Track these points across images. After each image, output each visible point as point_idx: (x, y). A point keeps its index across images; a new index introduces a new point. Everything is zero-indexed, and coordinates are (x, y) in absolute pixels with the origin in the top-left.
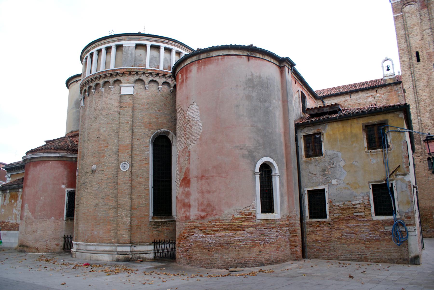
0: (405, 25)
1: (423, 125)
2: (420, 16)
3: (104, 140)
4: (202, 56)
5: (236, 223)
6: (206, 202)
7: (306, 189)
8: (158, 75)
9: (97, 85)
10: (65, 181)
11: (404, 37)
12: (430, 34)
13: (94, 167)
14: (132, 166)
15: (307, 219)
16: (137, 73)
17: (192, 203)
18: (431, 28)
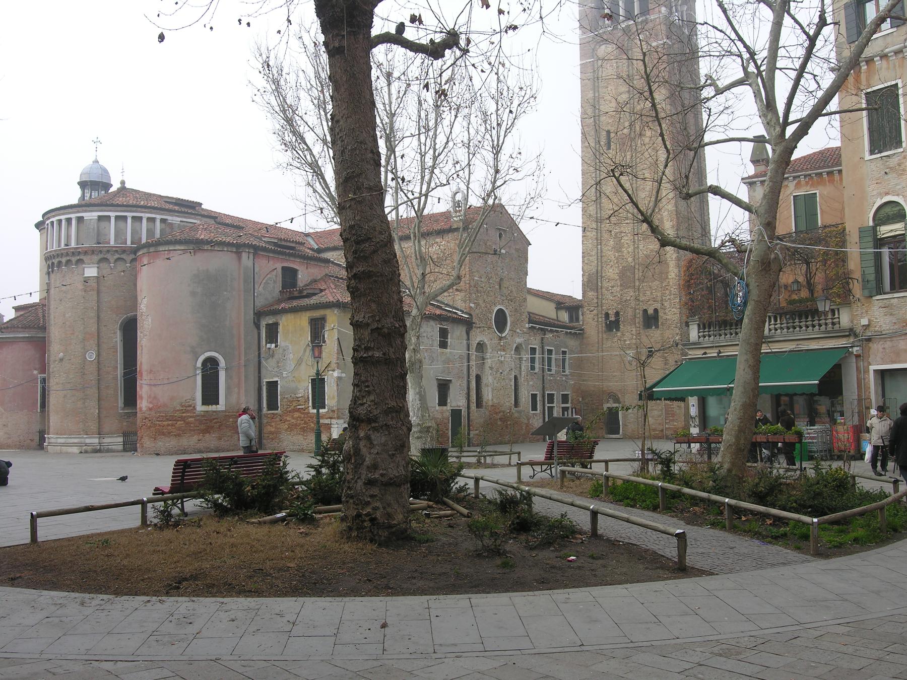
1: (604, 259)
4: (152, 249)
5: (177, 414)
7: (265, 380)
8: (124, 251)
9: (60, 262)
10: (37, 366)
14: (98, 355)
15: (265, 410)
16: (101, 252)
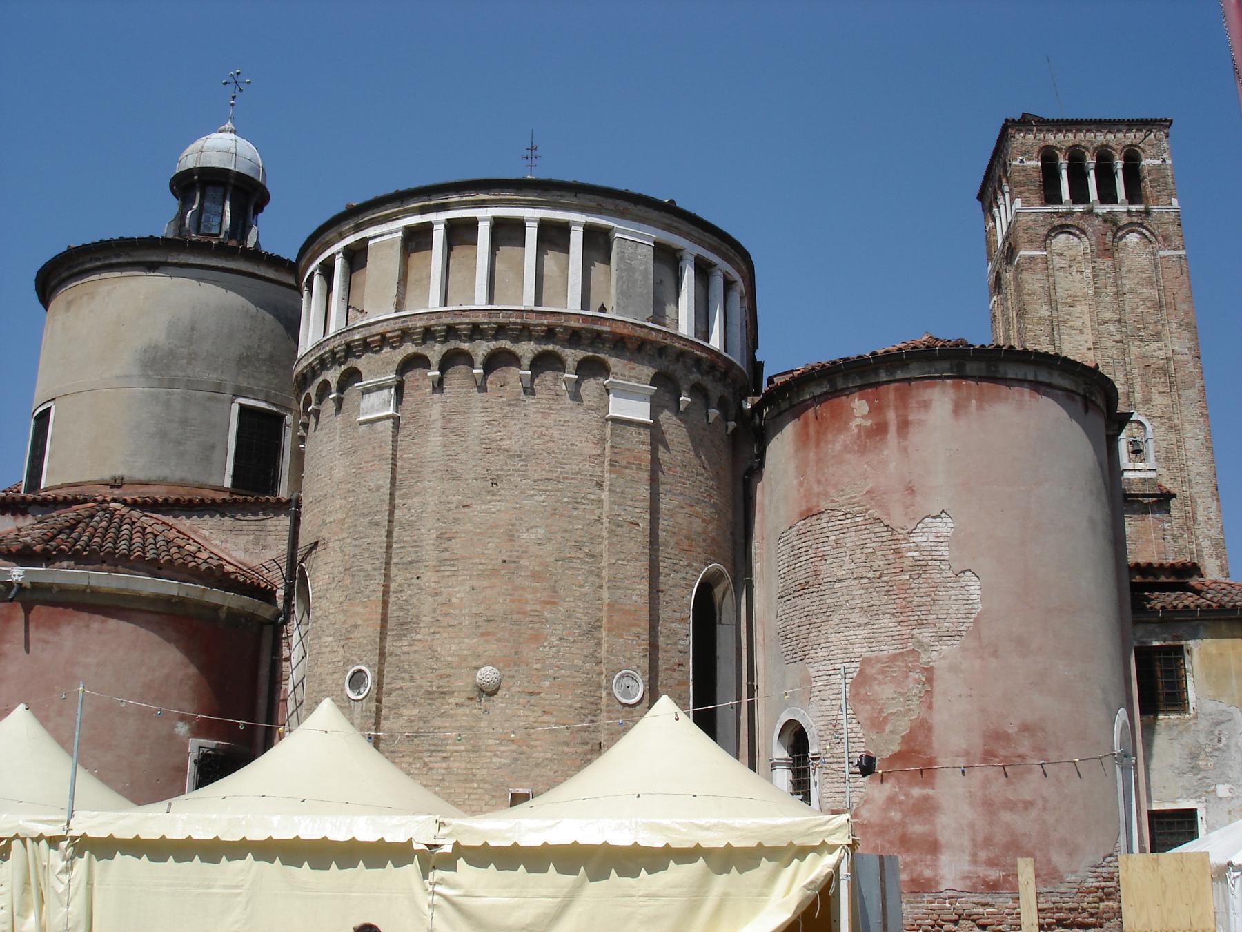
0: (1052, 292)
2: (1095, 276)
3: (535, 576)
6: (1000, 838)
11: (1049, 329)
12: (1118, 338)
13: (488, 674)
17: (944, 836)
18: (1119, 321)
